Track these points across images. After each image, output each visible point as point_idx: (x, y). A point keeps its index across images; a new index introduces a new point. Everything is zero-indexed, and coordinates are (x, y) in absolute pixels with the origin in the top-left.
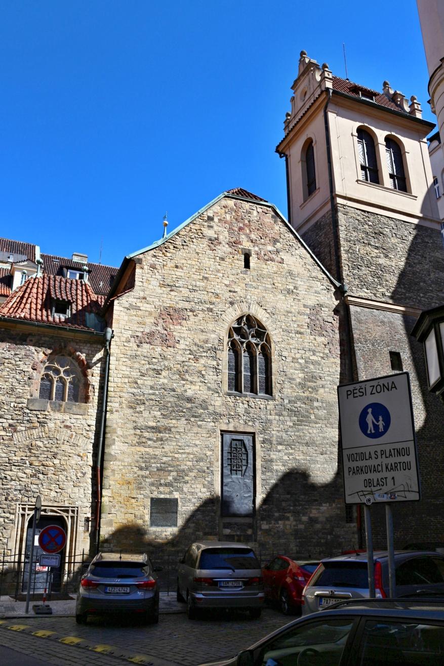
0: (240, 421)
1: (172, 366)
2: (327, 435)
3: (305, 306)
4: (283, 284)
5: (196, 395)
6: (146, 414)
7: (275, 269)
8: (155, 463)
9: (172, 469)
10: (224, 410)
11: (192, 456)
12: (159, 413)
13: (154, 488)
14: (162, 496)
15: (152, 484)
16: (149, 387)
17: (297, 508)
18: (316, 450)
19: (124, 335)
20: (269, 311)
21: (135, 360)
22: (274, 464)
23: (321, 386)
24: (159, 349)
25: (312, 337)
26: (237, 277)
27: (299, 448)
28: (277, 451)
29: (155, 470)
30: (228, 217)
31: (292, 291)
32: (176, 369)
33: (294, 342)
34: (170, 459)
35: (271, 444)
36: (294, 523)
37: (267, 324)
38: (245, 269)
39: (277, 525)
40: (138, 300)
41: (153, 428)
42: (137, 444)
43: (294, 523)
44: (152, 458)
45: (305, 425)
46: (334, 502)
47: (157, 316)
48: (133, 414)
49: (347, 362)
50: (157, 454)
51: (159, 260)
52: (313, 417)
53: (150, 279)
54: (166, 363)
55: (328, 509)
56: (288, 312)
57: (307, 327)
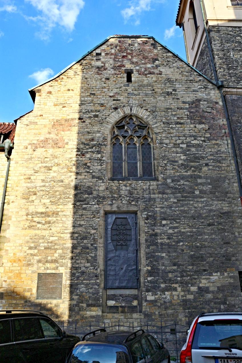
0: (123, 202)
1: (61, 162)
2: (213, 207)
3: (184, 102)
4: (162, 89)
5: (82, 183)
6: (37, 202)
7: (154, 79)
8: (43, 243)
9: (58, 247)
10: (108, 193)
11: (76, 235)
12: (49, 201)
13: (40, 265)
14: (49, 271)
15: (39, 261)
16: (41, 181)
17: (185, 278)
18: (202, 222)
19: (23, 144)
20: (149, 110)
21: (30, 161)
22: (159, 238)
23: (204, 165)
24: (51, 151)
25: (192, 126)
26: (120, 89)
27: (184, 222)
28: (161, 226)
29: (43, 248)
30: (113, 51)
31: (171, 93)
32: (64, 164)
33: (175, 131)
34: (57, 238)
35: (155, 219)
36: (182, 293)
37: (148, 120)
38: (127, 83)
39: (164, 296)
40: (36, 118)
41: (42, 213)
42: (28, 228)
43: (182, 293)
44: (40, 239)
45: (190, 201)
46: (226, 271)
47: (51, 126)
48: (26, 204)
49: (229, 141)
50: (45, 235)
51: (55, 88)
52: (197, 192)
53: (45, 102)
54: (56, 161)
55: (219, 278)
56: (169, 109)
57: (186, 118)
